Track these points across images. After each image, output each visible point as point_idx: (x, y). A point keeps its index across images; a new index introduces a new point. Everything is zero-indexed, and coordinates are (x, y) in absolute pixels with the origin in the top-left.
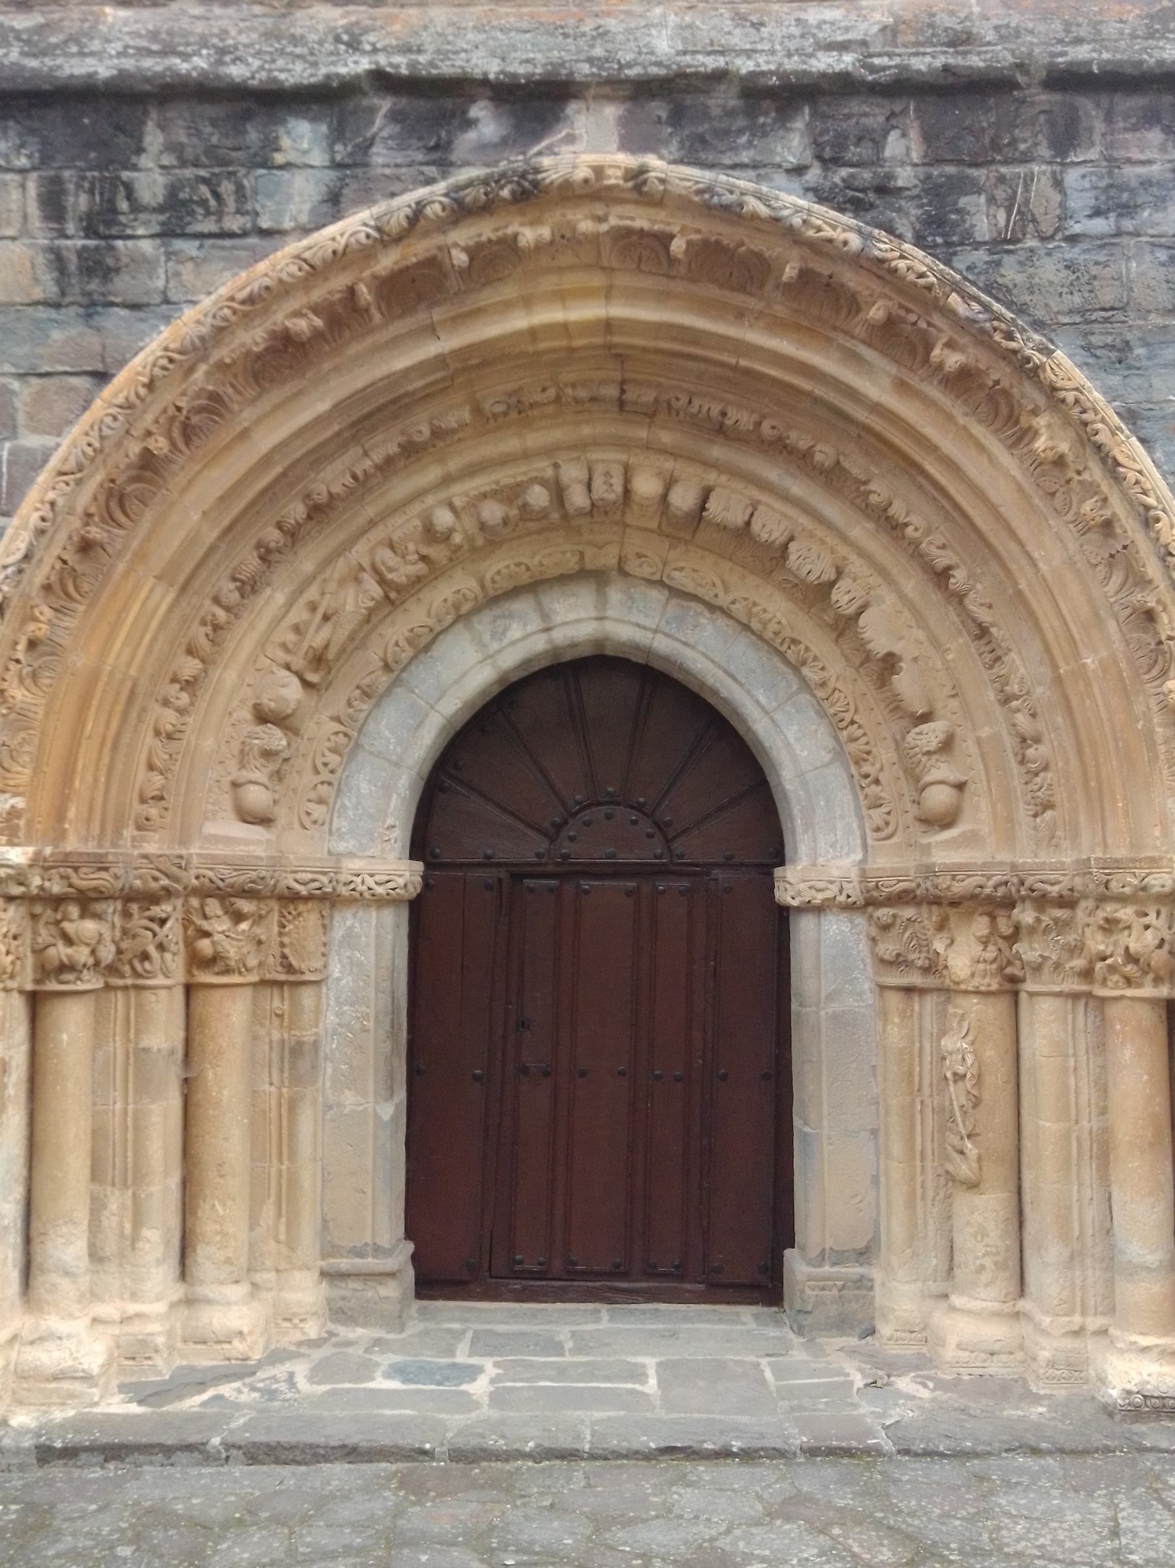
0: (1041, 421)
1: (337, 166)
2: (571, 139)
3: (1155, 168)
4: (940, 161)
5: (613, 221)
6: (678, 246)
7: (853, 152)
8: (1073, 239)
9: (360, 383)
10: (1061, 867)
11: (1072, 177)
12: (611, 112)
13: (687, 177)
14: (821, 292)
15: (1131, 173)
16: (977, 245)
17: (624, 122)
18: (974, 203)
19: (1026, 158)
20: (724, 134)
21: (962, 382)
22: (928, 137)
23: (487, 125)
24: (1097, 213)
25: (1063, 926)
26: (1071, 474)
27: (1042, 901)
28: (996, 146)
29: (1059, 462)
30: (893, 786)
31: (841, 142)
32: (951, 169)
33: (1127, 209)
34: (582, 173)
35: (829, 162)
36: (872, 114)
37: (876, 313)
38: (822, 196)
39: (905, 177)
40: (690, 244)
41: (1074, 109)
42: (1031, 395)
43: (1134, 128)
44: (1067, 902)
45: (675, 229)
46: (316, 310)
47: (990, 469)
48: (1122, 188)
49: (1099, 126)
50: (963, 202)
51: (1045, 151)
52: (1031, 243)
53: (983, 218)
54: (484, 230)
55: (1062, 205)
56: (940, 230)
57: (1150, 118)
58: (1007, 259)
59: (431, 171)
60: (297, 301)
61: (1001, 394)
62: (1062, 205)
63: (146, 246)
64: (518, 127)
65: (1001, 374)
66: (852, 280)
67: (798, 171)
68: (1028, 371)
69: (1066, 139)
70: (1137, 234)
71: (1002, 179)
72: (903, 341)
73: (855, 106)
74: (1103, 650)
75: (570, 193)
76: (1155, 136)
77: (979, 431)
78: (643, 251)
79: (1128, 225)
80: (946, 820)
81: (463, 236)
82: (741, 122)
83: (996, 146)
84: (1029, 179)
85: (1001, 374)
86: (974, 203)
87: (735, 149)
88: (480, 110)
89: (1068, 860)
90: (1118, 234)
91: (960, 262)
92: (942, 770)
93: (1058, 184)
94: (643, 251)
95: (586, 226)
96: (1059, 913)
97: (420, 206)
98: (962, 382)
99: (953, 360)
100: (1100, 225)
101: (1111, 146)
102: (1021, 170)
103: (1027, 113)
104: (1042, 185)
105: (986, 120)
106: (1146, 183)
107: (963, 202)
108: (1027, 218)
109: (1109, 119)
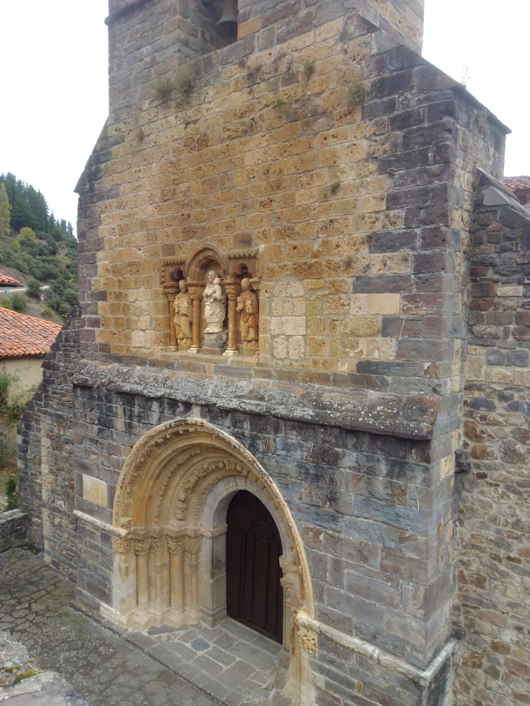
1: (160, 412)
2: (193, 413)
3: (294, 441)
4: (252, 431)
7: (239, 425)
8: (278, 455)
9: (175, 448)
11: (278, 440)
12: (199, 408)
13: (211, 426)
15: (290, 441)
16: (260, 452)
17: (201, 411)
18: (259, 442)
19: (269, 433)
20: (217, 417)
22: (251, 425)
23: (181, 408)
24: (283, 449)
28: (263, 429)
31: (236, 423)
32: (255, 433)
33: (289, 450)
34: (194, 422)
35: (235, 427)
36: (242, 417)
38: (233, 434)
39: (247, 433)
41: (278, 423)
43: (290, 430)
46: (162, 438)
48: (288, 445)
49: (283, 428)
50: (258, 441)
51: (272, 432)
52: (270, 454)
53: (261, 447)
55: (276, 446)
56: (253, 448)
57: (293, 428)
58: (266, 457)
59: (173, 416)
60: (158, 437)
62: (276, 446)
63: (136, 423)
64: (185, 409)
67: (229, 427)
69: (277, 430)
70: (290, 457)
71: (264, 438)
73: (239, 414)
76: (295, 432)
79: (289, 454)
82: (219, 415)
83: (263, 429)
84: (269, 439)
86: (259, 442)
87: (219, 420)
88: (180, 404)
90: (287, 456)
91: (257, 456)
93: (275, 441)
97: (171, 424)
100: (284, 453)
101: (286, 433)
102: (267, 436)
103: (270, 422)
104: (271, 441)
105: (262, 423)
106: (293, 444)
107: (258, 441)
108: (268, 449)
109: (285, 426)
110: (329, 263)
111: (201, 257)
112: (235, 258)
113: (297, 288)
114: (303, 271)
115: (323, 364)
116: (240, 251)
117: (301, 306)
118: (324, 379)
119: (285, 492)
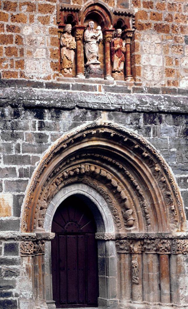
0: (157, 165)
5: (105, 131)
6: (112, 135)
10: (153, 234)
14: (129, 142)
21: (146, 159)
25: (153, 243)
26: (160, 173)
27: (151, 239)
29: (159, 171)
30: (122, 220)
37: (136, 147)
40: (114, 134)
42: (155, 161)
44: (154, 239)
45: (112, 132)
47: (147, 171)
54: (89, 132)
61: (152, 160)
65: (152, 158)
66: (135, 142)
68: (155, 156)
72: (139, 152)
74: (161, 200)
75: (101, 127)
77: (146, 165)
78: (106, 136)
80: (131, 226)
81: (86, 132)
85: (152, 158)
89: (155, 233)
92: (132, 218)
94: (106, 136)
95: (101, 131)
96: (153, 241)
98: (146, 159)
99: (146, 155)
110: (173, 26)
111: (97, 8)
112: (119, 14)
113: (156, 38)
114: (159, 28)
115: (172, 83)
116: (121, 10)
117: (159, 49)
118: (174, 91)
119: (167, 160)
